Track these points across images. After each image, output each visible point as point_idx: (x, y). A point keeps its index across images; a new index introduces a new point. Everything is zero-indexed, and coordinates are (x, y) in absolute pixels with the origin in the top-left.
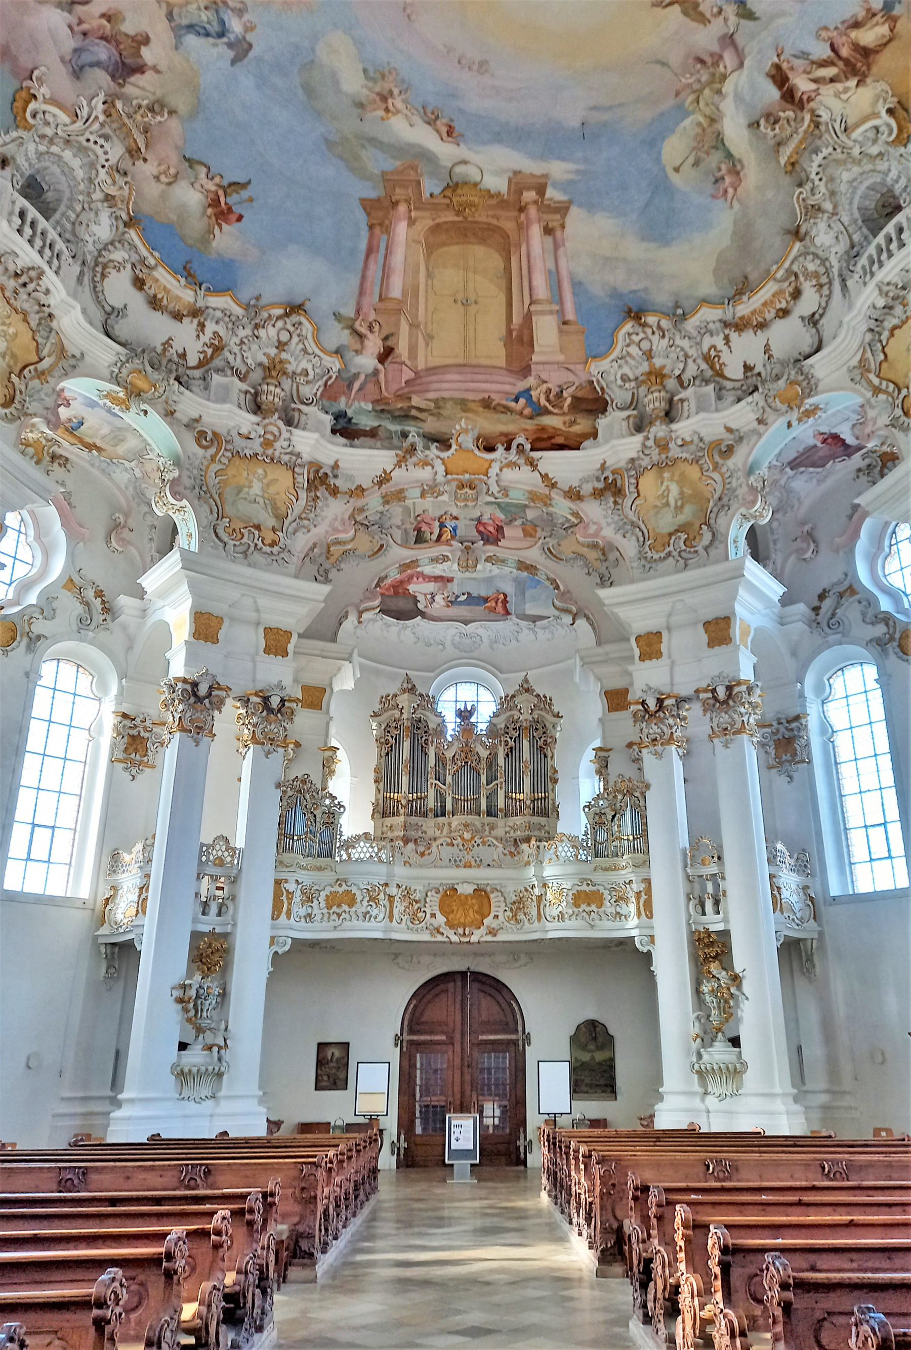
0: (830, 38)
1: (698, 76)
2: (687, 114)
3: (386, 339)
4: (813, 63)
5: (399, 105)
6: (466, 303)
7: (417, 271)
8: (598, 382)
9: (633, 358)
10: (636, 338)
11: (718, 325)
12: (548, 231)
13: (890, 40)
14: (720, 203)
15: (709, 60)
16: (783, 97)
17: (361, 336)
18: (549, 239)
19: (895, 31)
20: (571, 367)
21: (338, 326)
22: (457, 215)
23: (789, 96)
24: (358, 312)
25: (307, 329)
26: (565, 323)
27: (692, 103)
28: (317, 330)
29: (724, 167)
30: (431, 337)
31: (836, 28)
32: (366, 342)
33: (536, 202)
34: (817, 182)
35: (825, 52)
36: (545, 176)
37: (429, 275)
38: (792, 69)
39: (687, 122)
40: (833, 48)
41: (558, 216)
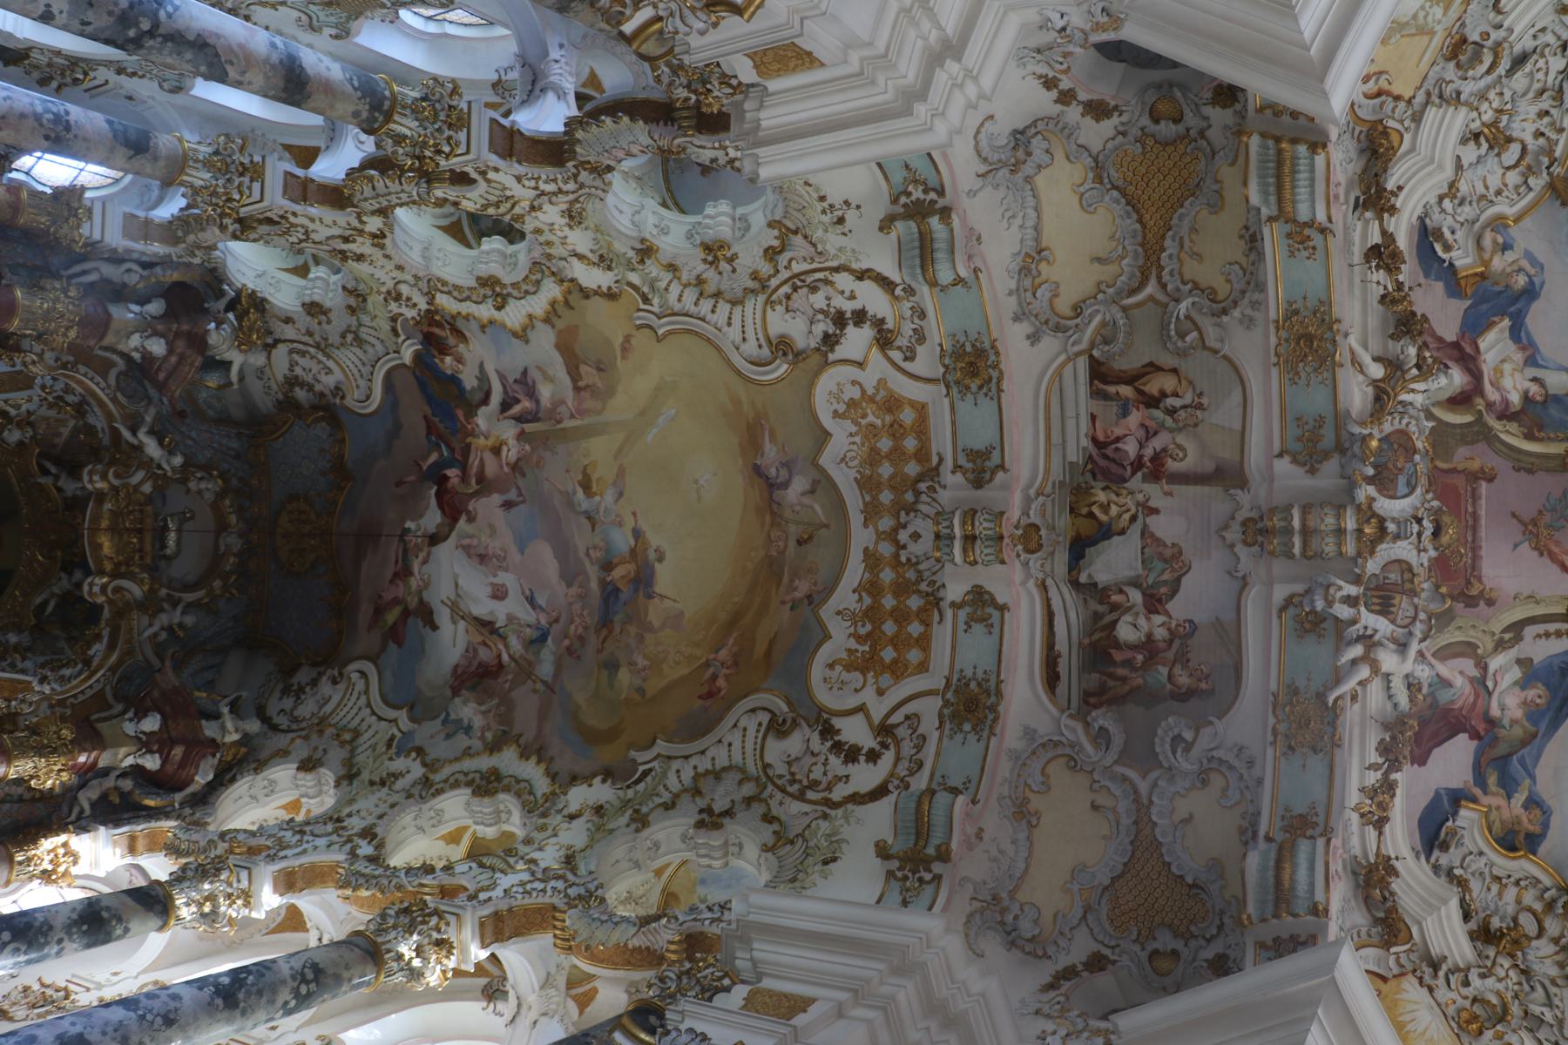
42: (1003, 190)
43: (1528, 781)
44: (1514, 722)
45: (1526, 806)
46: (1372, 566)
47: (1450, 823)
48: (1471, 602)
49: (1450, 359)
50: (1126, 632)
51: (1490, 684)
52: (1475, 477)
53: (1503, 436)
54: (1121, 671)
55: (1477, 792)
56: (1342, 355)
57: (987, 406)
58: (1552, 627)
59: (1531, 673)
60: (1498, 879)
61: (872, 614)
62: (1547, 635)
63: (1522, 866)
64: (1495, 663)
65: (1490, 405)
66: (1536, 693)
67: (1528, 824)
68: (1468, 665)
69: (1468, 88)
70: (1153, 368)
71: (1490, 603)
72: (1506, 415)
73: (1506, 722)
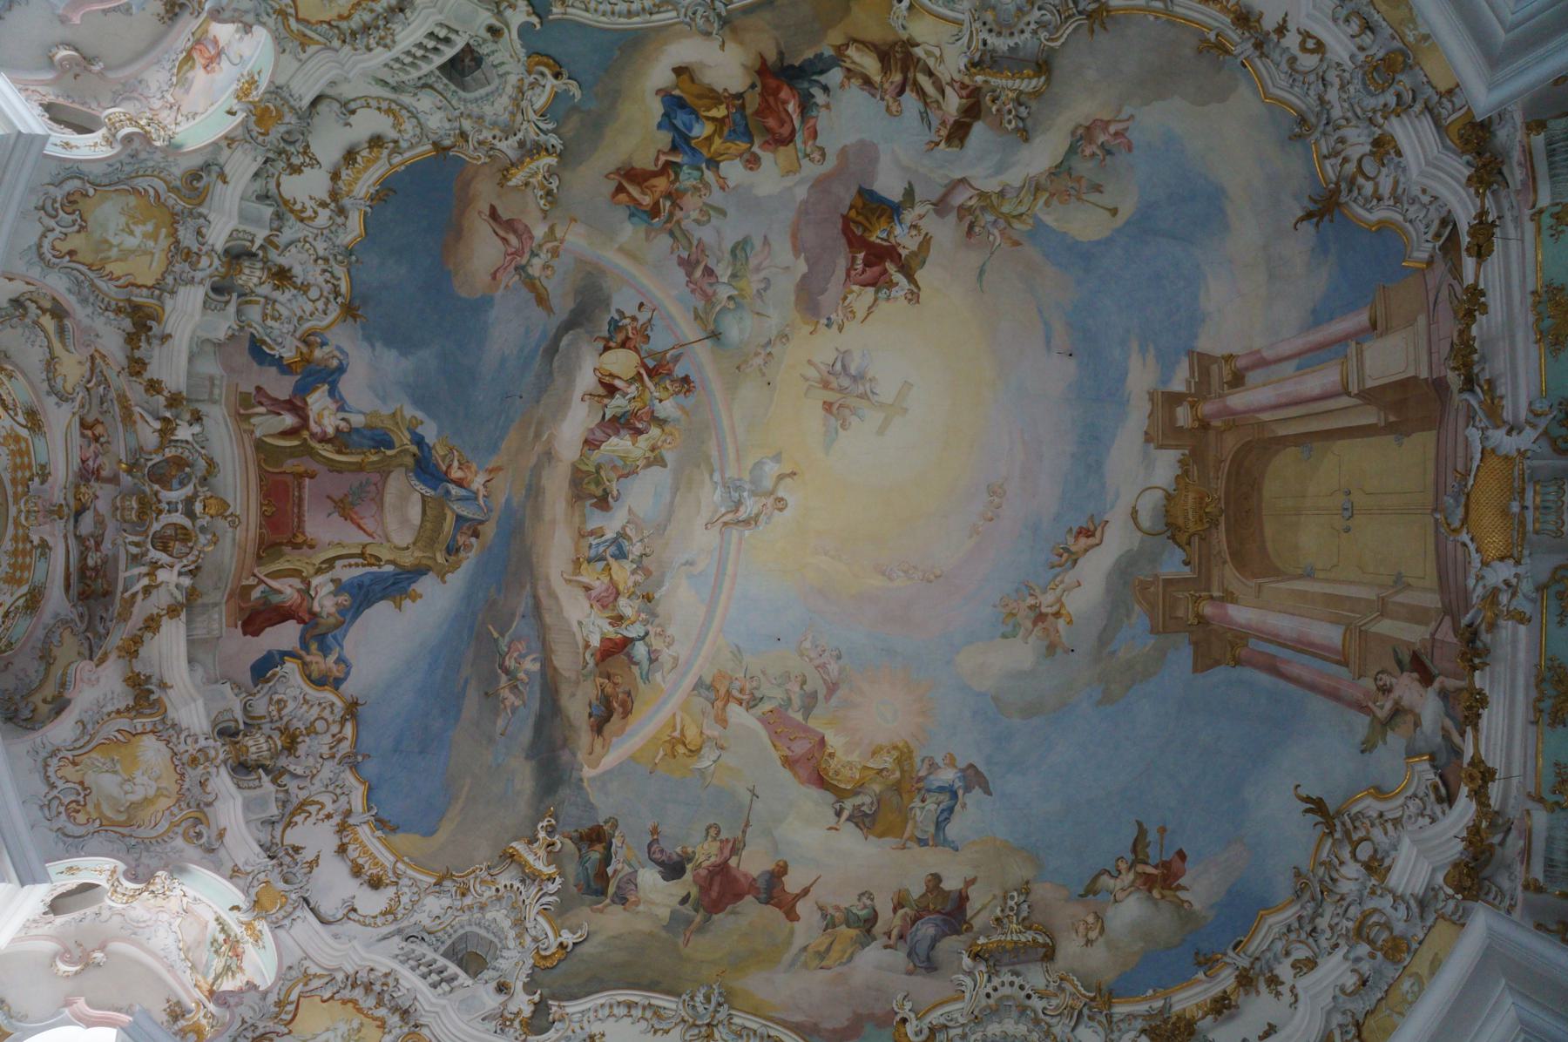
0: (895, 100)
1: (989, 226)
2: (1039, 224)
3: (1399, 663)
4: (926, 104)
5: (1049, 598)
6: (1349, 511)
7: (1303, 595)
8: (1438, 235)
9: (1396, 183)
10: (1368, 188)
11: (1276, 55)
12: (1237, 380)
13: (855, 41)
14: (1133, 135)
15: (969, 218)
16: (977, 117)
17: (1398, 711)
18: (1252, 377)
19: (844, 41)
20: (1432, 299)
21: (1381, 751)
22: (1217, 525)
23: (973, 110)
24: (1362, 708)
25: (1372, 806)
26: (1374, 326)
27: (1024, 222)
28: (1379, 792)
29: (1088, 152)
30: (1399, 576)
31: (882, 99)
32: (1405, 703)
33: (1193, 406)
34: (1033, 26)
35: (910, 97)
36: (1152, 396)
37: (1309, 575)
38: (943, 123)
39: (1049, 220)
40: (901, 92)
41: (1214, 368)
42: (20, 330)
43: (338, 649)
44: (329, 615)
45: (337, 662)
46: (156, 527)
47: (278, 669)
48: (297, 546)
49: (283, 409)
50: (90, 562)
51: (312, 593)
52: (300, 476)
53: (324, 453)
54: (89, 582)
55: (303, 653)
56: (137, 417)
57: (43, 439)
58: (353, 561)
59: (339, 587)
60: (306, 701)
61: (15, 553)
62: (350, 565)
63: (328, 695)
64: (315, 582)
65: (313, 435)
66: (344, 599)
67: (336, 671)
68: (297, 583)
69: (199, 275)
70: (97, 421)
71: (311, 547)
72: (324, 439)
73: (324, 615)
